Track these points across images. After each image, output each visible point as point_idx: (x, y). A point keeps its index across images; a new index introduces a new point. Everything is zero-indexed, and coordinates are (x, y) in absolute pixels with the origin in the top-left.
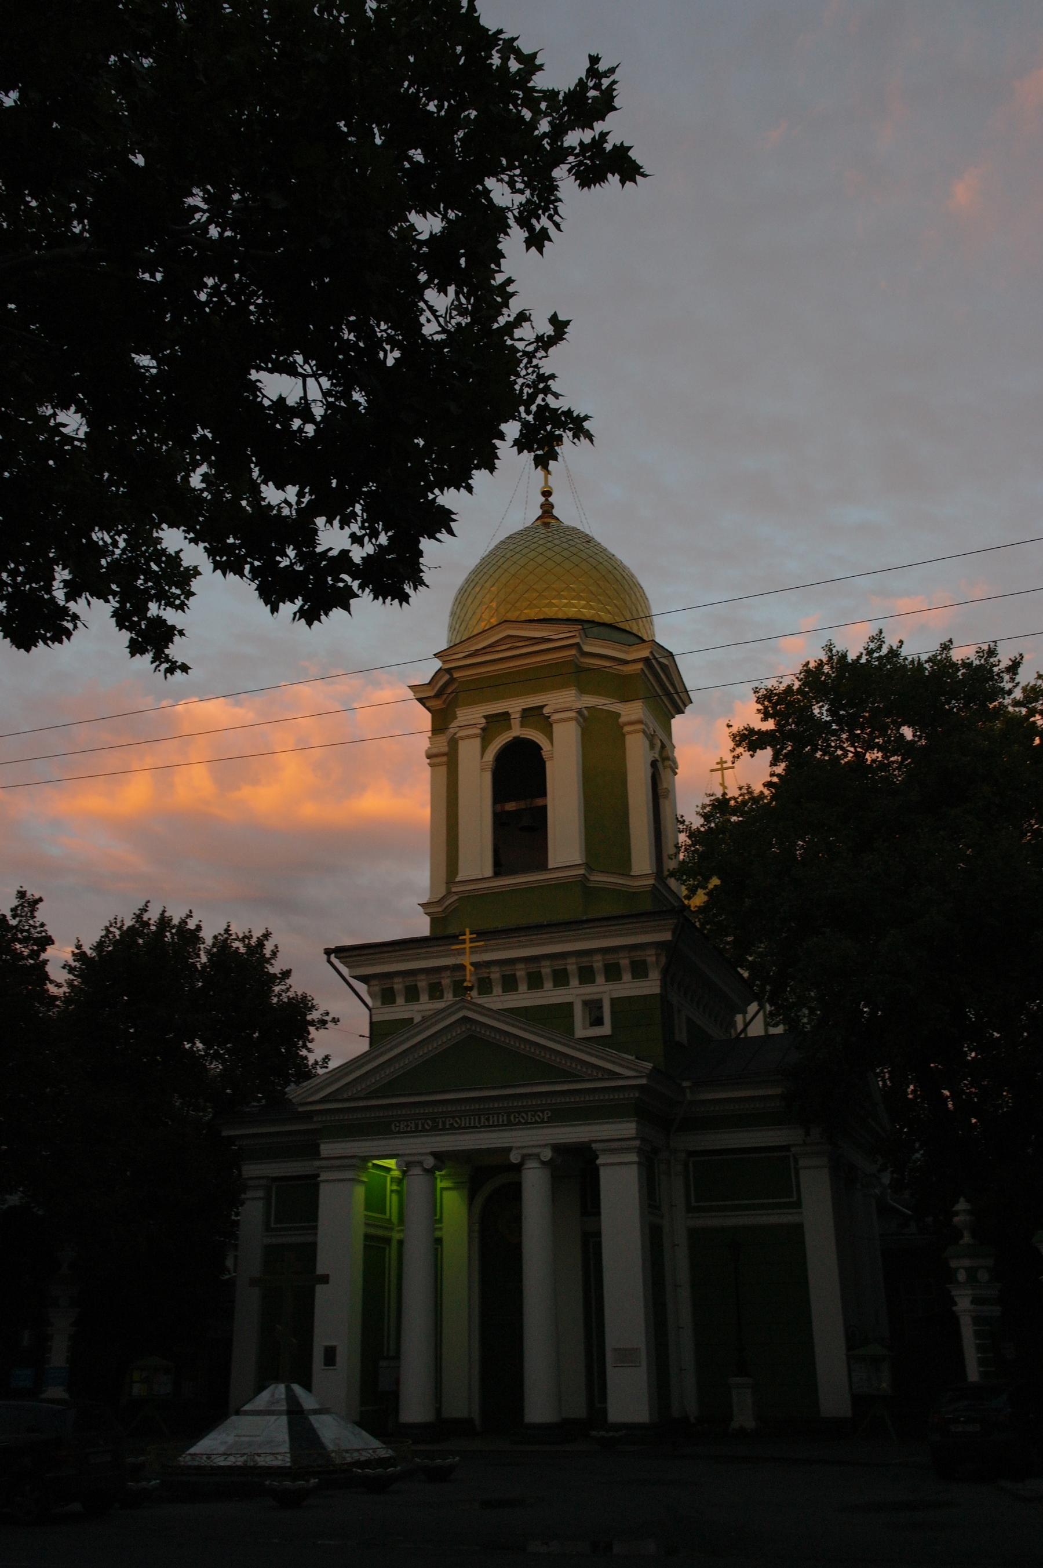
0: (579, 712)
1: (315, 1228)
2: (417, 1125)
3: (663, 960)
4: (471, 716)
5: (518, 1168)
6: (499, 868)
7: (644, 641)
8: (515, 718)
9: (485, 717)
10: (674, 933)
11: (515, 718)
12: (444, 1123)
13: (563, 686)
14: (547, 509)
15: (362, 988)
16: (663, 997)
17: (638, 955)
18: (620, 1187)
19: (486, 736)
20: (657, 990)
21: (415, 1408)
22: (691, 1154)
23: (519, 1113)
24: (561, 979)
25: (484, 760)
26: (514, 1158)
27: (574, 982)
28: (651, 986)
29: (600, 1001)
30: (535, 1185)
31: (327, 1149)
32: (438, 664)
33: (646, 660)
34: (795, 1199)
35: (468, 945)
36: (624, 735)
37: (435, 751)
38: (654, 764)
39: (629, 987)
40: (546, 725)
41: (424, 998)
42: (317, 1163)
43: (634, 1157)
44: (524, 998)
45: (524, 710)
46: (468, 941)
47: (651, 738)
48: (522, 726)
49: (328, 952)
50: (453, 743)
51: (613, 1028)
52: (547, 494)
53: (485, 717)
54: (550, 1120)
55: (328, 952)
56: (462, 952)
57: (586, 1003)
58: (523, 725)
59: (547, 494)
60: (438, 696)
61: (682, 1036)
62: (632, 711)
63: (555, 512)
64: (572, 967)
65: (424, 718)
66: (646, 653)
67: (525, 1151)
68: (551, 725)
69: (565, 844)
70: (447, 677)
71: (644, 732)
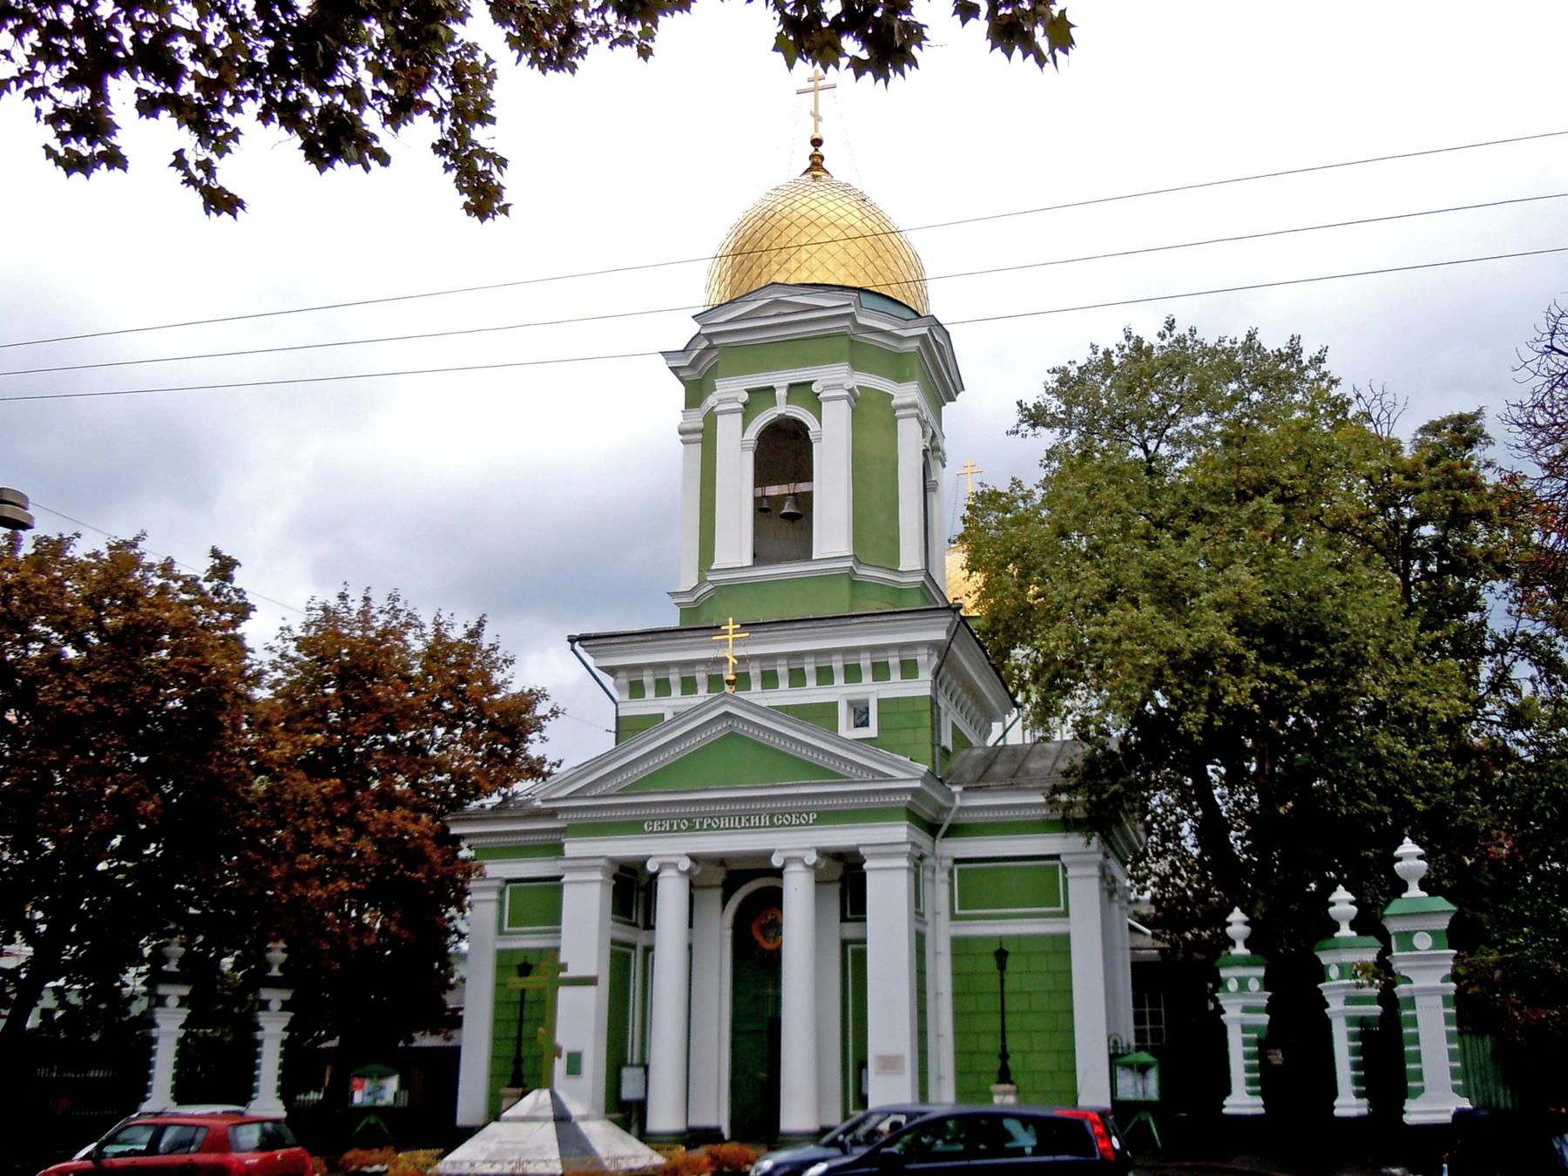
0: (851, 391)
1: (559, 931)
2: (671, 825)
3: (935, 661)
4: (730, 390)
5: (778, 873)
6: (759, 558)
7: (919, 316)
8: (781, 393)
9: (748, 391)
10: (948, 631)
11: (781, 393)
12: (701, 824)
13: (835, 359)
14: (816, 163)
15: (608, 680)
16: (933, 701)
17: (908, 655)
18: (887, 890)
19: (748, 411)
20: (928, 692)
21: (664, 1117)
22: (957, 861)
24: (825, 676)
26: (776, 862)
27: (839, 680)
28: (921, 686)
29: (867, 701)
30: (798, 893)
31: (572, 848)
32: (695, 328)
33: (923, 338)
35: (730, 637)
36: (896, 419)
37: (688, 426)
38: (925, 452)
39: (896, 688)
40: (815, 404)
41: (676, 692)
42: (561, 863)
43: (904, 863)
44: (785, 695)
45: (791, 386)
47: (923, 423)
48: (789, 401)
49: (572, 640)
50: (711, 419)
51: (879, 730)
52: (817, 143)
53: (748, 391)
55: (572, 640)
56: (723, 644)
57: (850, 704)
58: (789, 400)
59: (817, 143)
60: (693, 365)
61: (947, 741)
62: (907, 393)
63: (825, 165)
64: (837, 664)
65: (677, 391)
66: (924, 331)
67: (788, 854)
69: (832, 534)
70: (705, 344)
71: (918, 417)
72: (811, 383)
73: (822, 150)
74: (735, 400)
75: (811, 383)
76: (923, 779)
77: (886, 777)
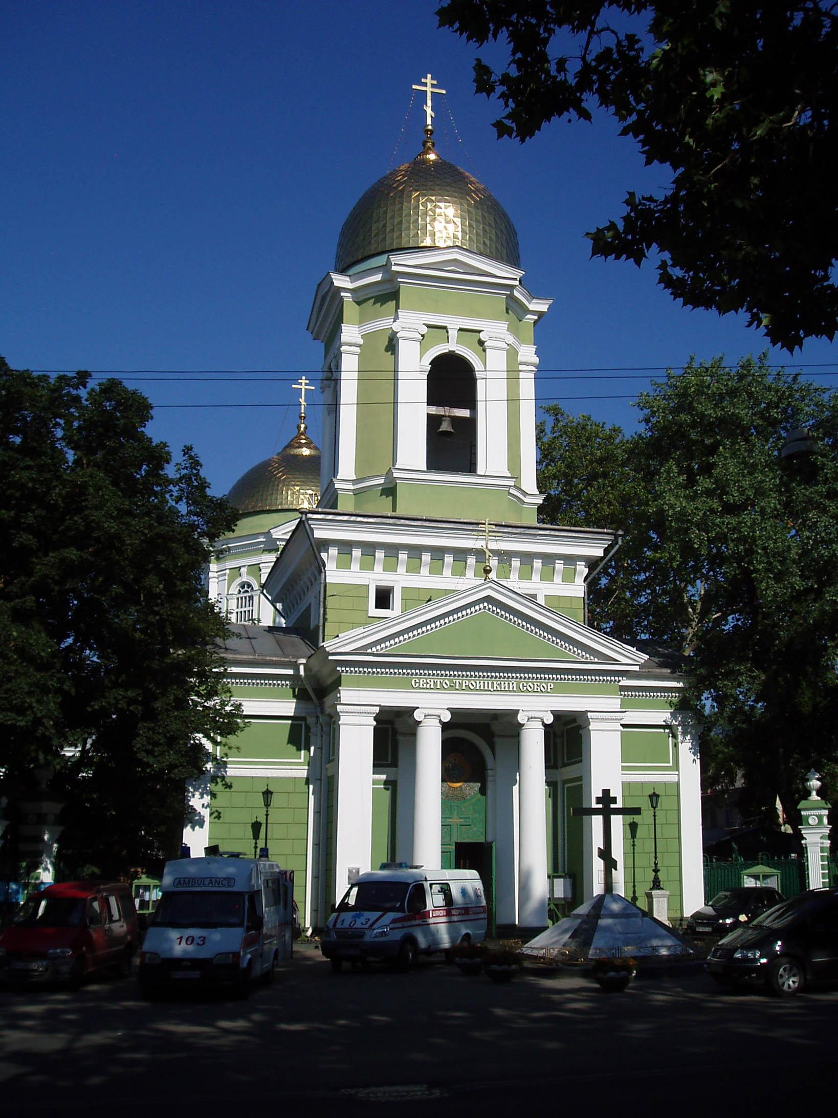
8: (453, 334)
9: (429, 326)
10: (606, 551)
11: (453, 334)
45: (461, 330)
68: (484, 350)
72: (480, 331)
74: (416, 330)
75: (480, 331)
76: (641, 666)
77: (615, 661)
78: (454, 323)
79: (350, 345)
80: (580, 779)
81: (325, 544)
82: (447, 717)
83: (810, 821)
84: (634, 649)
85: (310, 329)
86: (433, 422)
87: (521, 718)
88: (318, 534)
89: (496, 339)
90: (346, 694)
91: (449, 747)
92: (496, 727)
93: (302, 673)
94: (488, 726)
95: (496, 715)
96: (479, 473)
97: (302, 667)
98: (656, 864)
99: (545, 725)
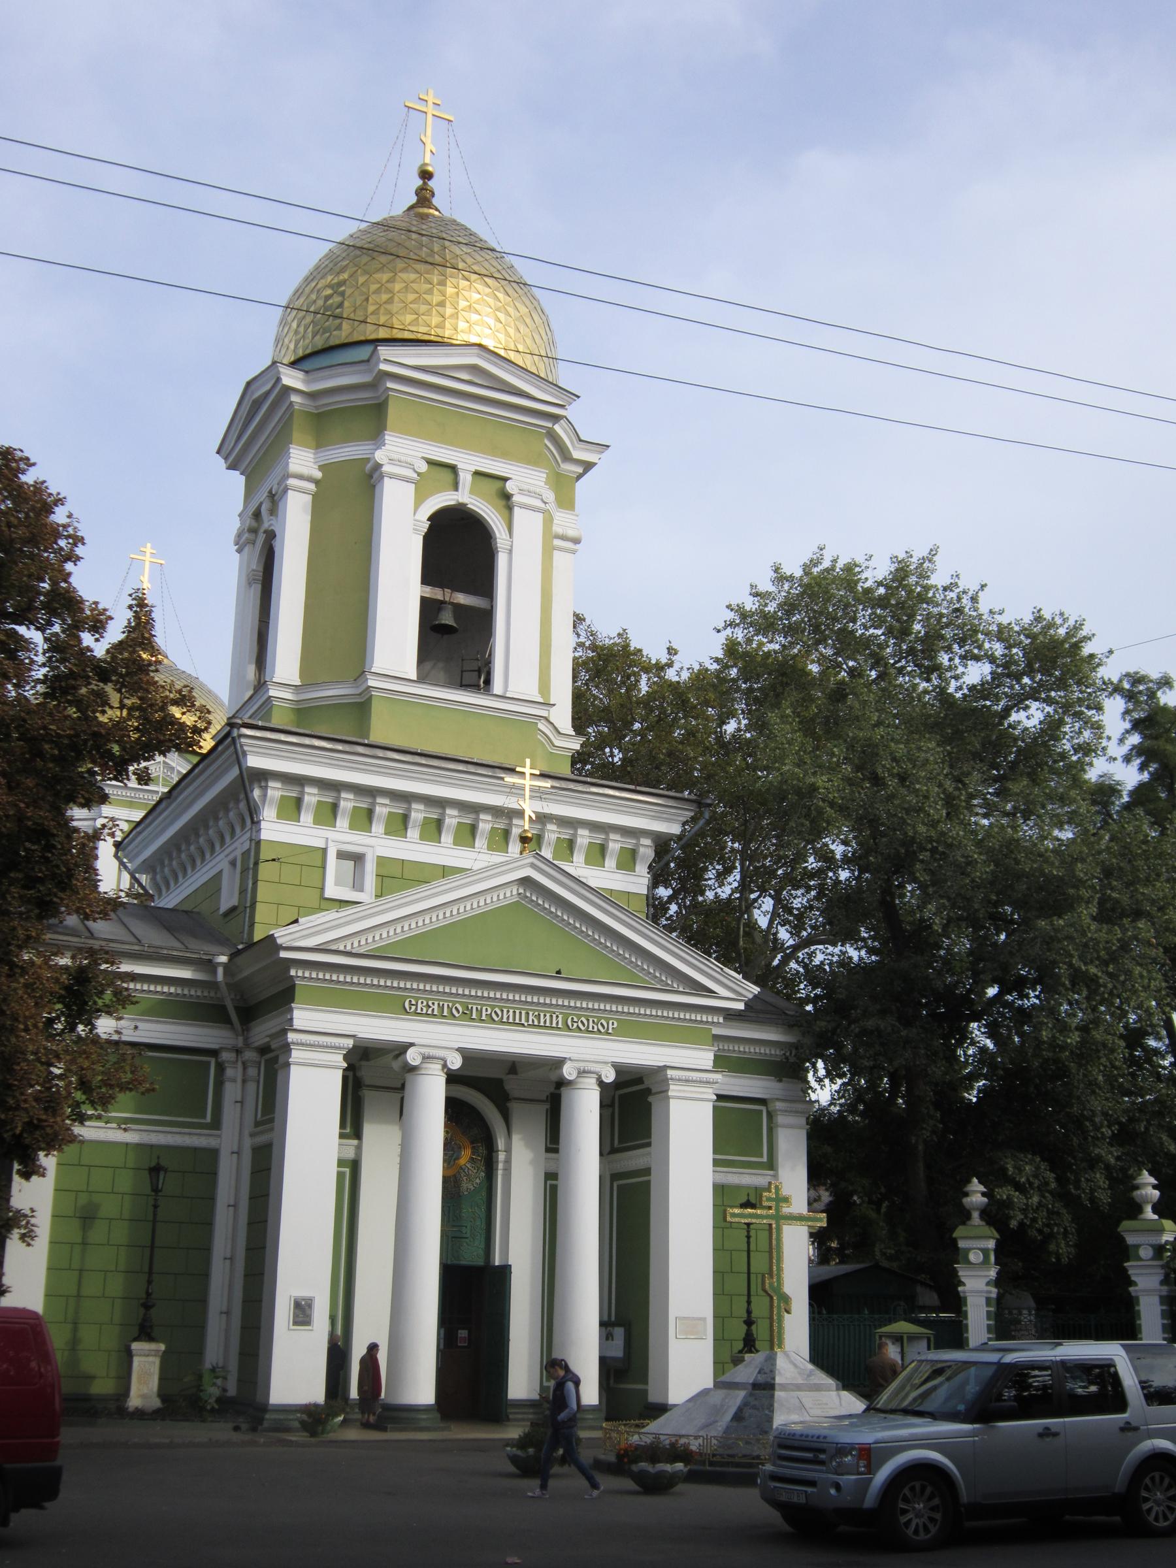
2: (441, 1008)
8: (465, 478)
9: (431, 463)
14: (424, 197)
23: (579, 1017)
25: (418, 517)
34: (765, 1159)
45: (477, 474)
46: (528, 776)
52: (426, 175)
54: (618, 1032)
56: (517, 790)
68: (510, 508)
73: (431, 183)
75: (505, 479)
77: (710, 992)
78: (468, 462)
79: (301, 477)
80: (647, 1171)
81: (262, 776)
82: (456, 1062)
83: (972, 1257)
84: (740, 977)
85: (224, 451)
86: (427, 606)
87: (568, 1072)
88: (254, 761)
89: (529, 493)
90: (303, 1017)
91: (456, 1111)
92: (512, 1086)
93: (220, 975)
94: (499, 1082)
95: (514, 1065)
96: (495, 692)
97: (220, 971)
98: (749, 1312)
99: (601, 1083)
